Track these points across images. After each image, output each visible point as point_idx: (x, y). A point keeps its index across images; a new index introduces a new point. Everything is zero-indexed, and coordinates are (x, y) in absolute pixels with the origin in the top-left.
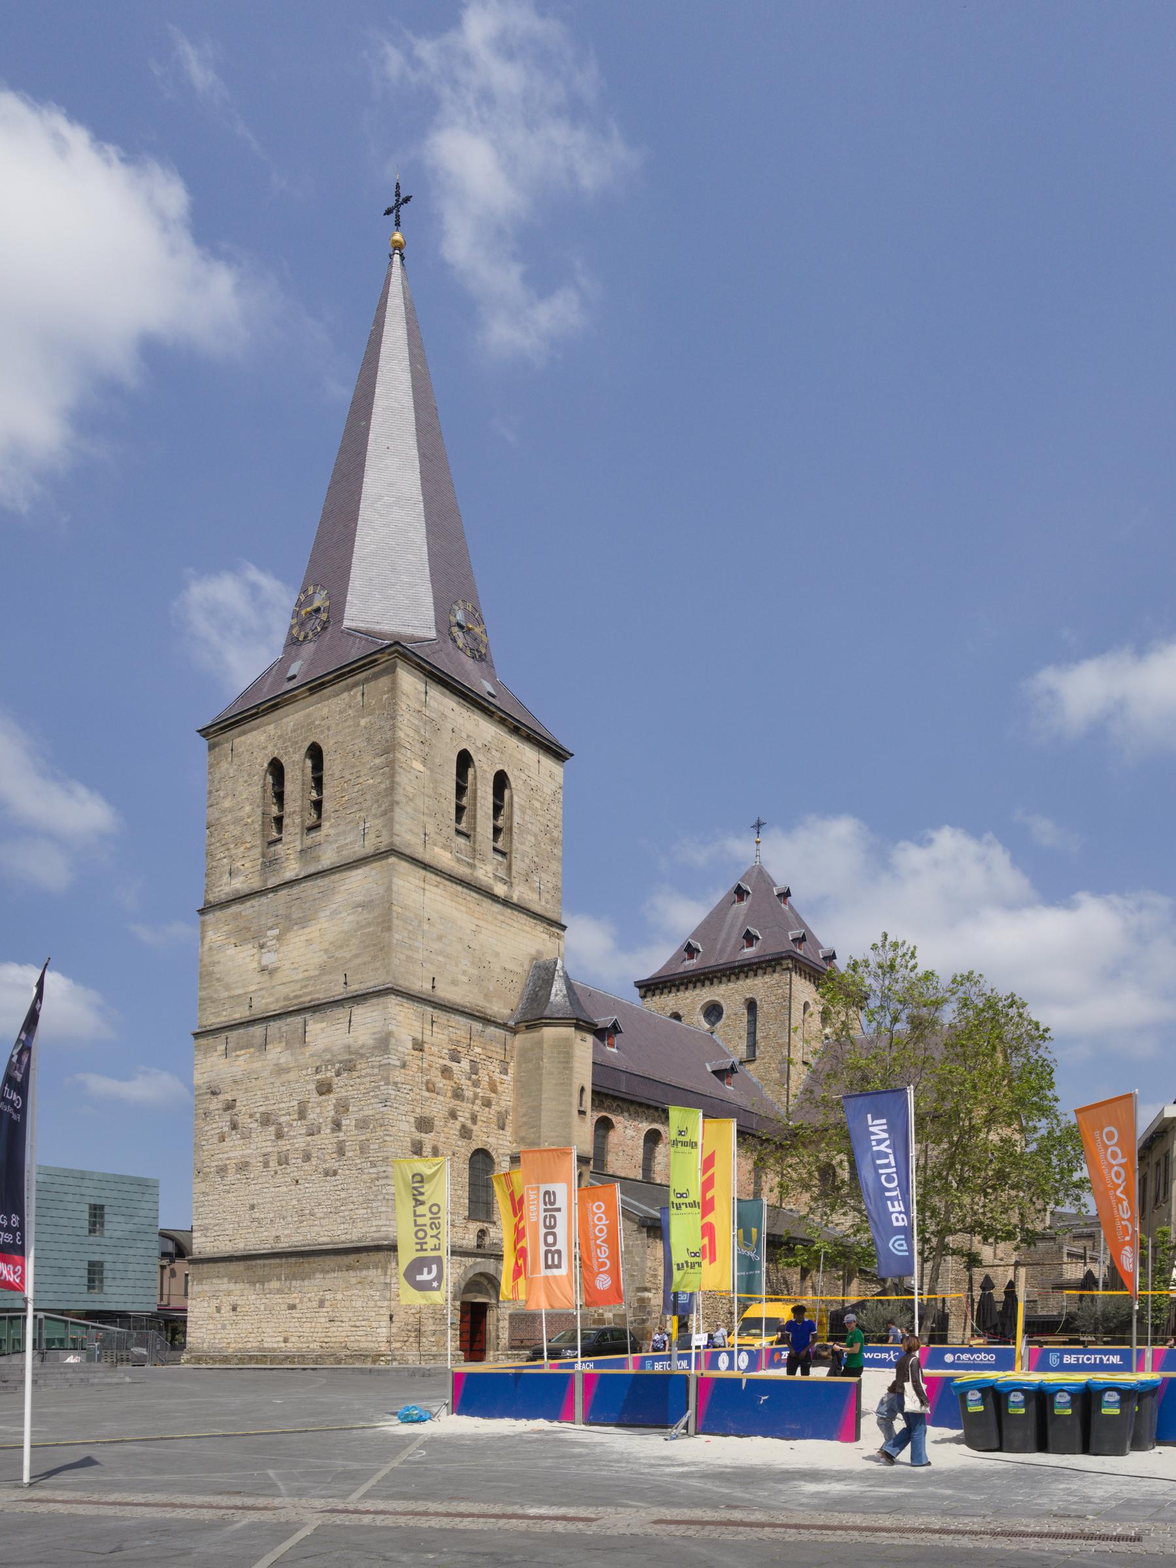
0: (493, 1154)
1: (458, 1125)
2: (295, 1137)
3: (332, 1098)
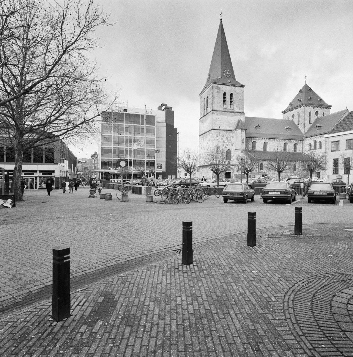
0: (231, 150)
1: (224, 146)
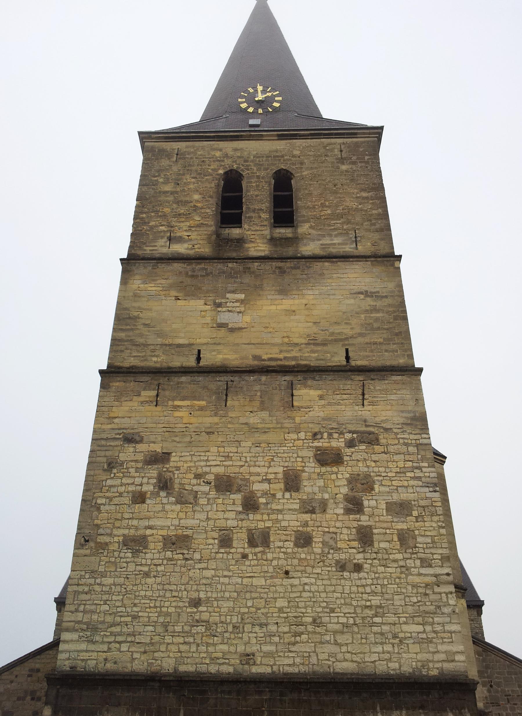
2: (280, 511)
3: (344, 473)
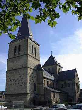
3: (21, 78)
